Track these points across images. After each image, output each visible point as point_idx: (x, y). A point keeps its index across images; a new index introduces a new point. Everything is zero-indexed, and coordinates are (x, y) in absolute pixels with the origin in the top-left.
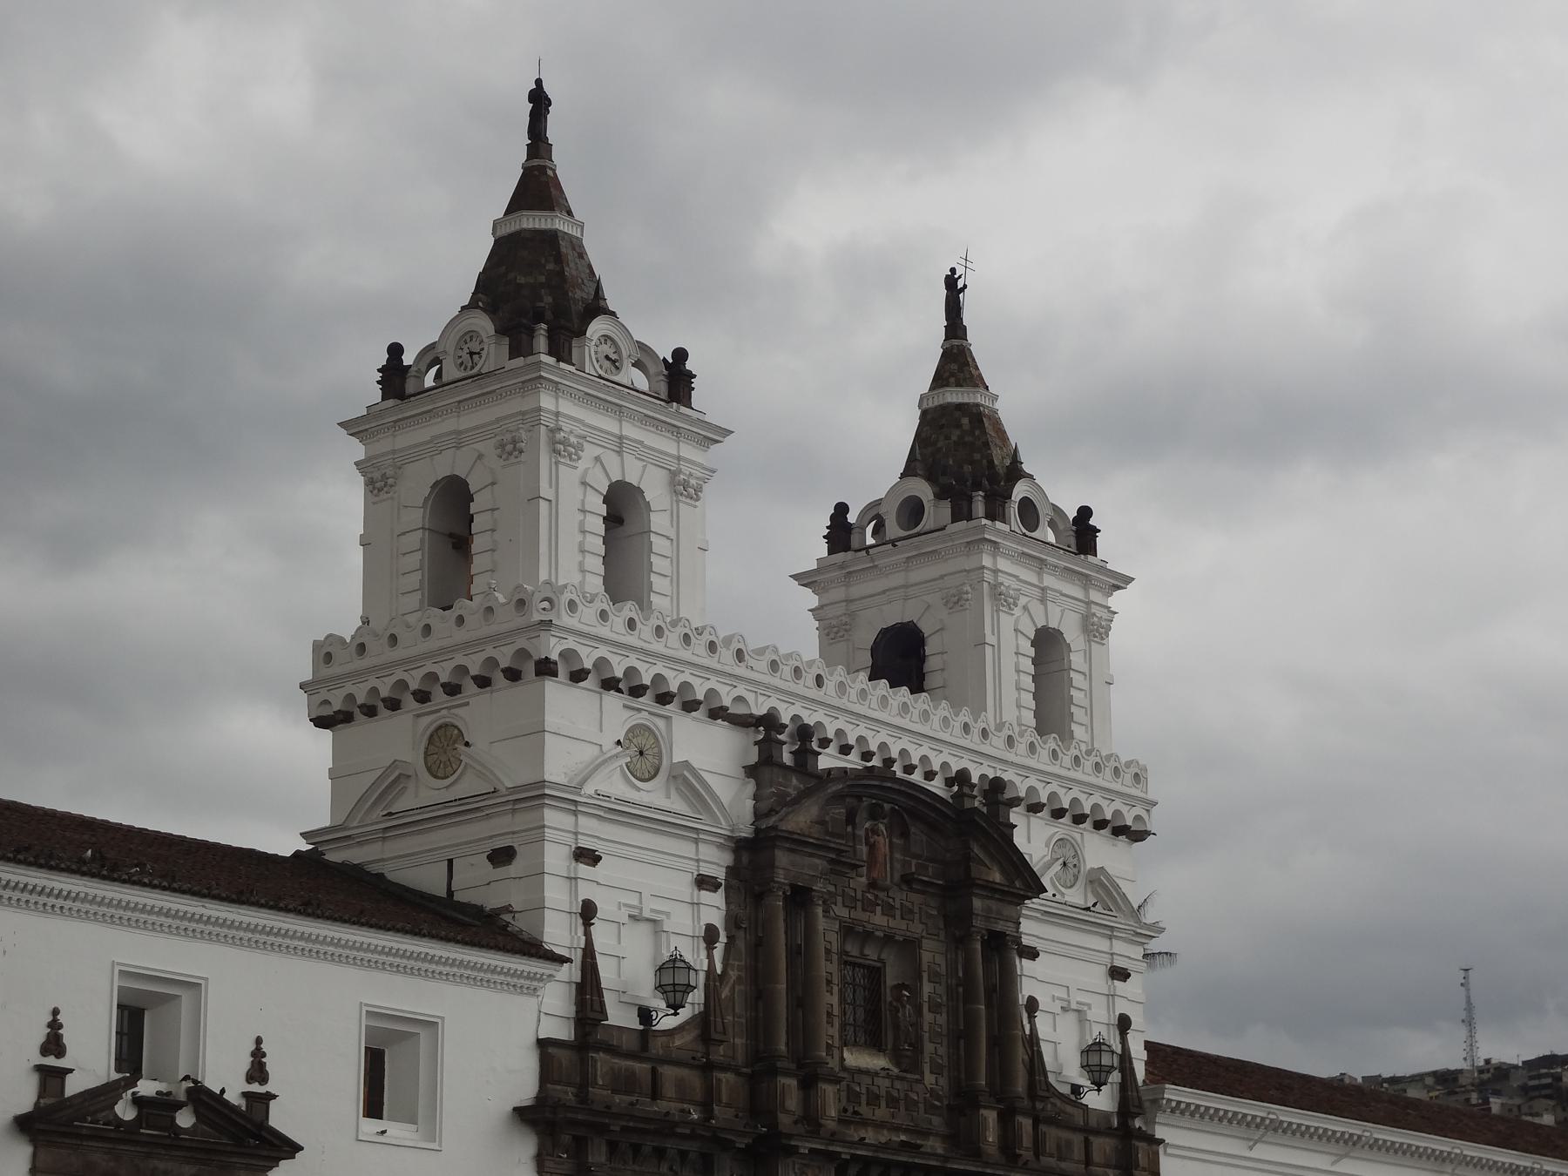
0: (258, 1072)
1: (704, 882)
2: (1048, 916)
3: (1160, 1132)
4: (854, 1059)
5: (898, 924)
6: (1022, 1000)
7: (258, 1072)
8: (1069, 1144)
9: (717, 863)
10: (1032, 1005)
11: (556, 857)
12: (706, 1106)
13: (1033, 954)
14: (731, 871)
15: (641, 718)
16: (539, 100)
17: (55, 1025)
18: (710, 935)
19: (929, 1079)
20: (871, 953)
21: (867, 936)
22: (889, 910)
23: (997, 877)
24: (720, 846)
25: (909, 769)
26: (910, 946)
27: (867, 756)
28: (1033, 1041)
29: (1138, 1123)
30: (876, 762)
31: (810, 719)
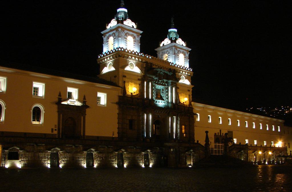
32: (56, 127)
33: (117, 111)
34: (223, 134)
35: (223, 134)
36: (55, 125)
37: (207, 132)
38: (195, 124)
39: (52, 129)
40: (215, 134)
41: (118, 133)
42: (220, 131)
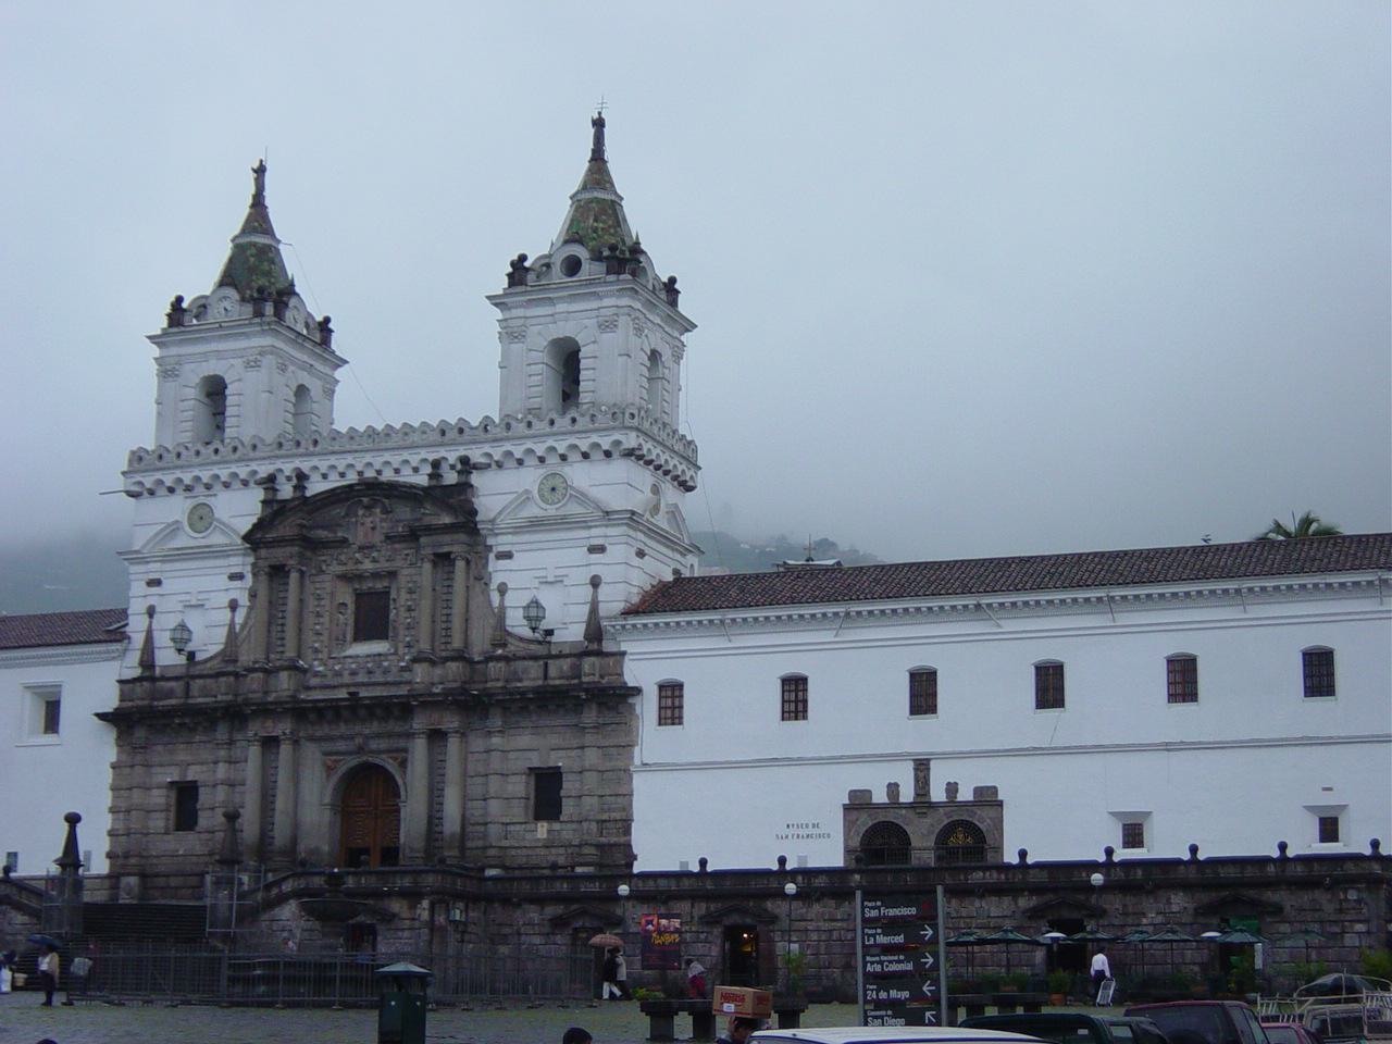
1: (233, 577)
2: (517, 530)
3: (623, 649)
5: (384, 565)
6: (494, 586)
8: (525, 671)
9: (243, 563)
10: (503, 589)
11: (138, 588)
12: (216, 697)
13: (508, 555)
14: (254, 565)
15: (202, 500)
16: (260, 171)
18: (233, 606)
20: (379, 585)
21: (360, 577)
22: (374, 561)
23: (447, 519)
24: (244, 555)
25: (397, 471)
26: (392, 575)
27: (360, 473)
28: (502, 608)
29: (608, 646)
30: (369, 474)
33: (111, 753)
34: (952, 789)
35: (952, 789)
37: (73, 820)
38: (637, 750)
40: (858, 804)
41: (109, 855)
42: (922, 767)
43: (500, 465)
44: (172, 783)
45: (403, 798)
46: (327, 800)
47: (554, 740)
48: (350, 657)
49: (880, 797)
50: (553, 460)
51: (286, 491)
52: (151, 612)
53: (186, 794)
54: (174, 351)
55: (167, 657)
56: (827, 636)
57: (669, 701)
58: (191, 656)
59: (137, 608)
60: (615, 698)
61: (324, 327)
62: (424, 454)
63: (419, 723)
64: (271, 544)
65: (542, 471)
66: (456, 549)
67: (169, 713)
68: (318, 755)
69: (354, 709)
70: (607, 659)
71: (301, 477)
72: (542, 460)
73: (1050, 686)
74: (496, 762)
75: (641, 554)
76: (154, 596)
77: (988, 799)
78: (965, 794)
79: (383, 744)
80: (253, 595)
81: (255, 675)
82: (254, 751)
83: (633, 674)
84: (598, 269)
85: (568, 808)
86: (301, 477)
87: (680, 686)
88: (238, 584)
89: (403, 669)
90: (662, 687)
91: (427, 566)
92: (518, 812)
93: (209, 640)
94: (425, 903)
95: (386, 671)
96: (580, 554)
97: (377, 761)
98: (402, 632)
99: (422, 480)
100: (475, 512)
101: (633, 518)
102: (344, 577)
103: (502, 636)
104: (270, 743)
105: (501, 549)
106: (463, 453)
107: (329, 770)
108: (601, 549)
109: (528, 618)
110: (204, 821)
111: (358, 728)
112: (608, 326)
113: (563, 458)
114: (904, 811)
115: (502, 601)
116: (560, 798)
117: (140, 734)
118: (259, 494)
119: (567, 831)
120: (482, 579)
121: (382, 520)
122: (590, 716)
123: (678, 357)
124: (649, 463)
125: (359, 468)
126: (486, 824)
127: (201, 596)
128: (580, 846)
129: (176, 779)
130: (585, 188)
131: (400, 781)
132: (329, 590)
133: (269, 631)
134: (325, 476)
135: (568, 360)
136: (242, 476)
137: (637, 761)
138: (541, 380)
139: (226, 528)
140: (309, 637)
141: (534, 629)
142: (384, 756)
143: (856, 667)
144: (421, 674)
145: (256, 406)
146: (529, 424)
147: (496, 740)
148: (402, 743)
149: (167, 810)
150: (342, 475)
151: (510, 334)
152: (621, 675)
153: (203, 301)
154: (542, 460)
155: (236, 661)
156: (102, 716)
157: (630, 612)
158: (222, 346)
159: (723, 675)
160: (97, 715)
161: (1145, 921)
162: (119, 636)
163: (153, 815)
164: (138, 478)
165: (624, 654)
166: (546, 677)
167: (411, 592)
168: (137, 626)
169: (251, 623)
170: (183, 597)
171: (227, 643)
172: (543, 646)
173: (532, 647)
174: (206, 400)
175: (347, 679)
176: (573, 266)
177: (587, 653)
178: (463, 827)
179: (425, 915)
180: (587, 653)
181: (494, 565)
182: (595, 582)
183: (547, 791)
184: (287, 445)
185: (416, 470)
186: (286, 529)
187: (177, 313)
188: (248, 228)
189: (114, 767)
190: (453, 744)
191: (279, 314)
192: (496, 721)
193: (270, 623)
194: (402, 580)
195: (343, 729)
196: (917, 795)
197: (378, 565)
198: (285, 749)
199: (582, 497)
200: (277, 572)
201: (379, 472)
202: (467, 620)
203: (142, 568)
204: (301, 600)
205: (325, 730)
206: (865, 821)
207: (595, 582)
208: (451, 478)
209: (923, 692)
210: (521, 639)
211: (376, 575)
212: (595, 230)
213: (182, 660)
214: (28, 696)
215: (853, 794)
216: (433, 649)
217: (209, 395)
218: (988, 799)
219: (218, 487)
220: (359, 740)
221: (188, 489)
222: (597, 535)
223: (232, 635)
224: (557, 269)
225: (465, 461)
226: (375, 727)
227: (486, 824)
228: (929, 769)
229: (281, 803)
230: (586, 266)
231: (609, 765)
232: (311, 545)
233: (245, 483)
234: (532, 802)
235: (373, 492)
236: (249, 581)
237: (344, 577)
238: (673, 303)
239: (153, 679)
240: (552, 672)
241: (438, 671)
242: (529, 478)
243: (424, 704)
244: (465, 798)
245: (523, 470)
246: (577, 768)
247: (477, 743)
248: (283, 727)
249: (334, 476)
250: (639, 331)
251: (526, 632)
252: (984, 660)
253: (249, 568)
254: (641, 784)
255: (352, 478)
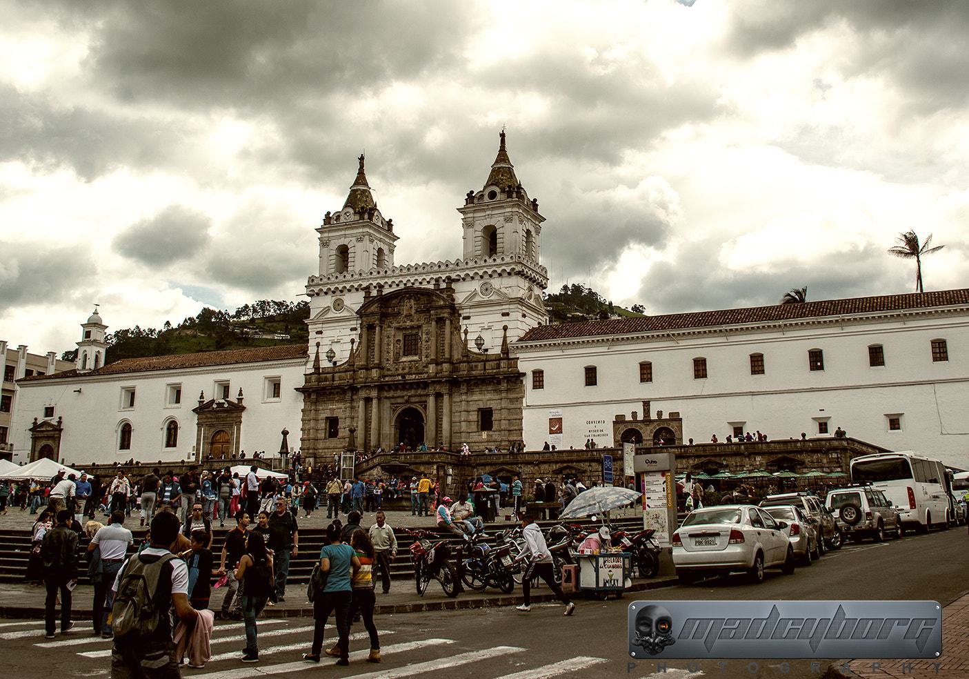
0: (241, 394)
1: (352, 330)
2: (471, 307)
4: (404, 359)
7: (241, 394)
8: (476, 366)
9: (356, 323)
10: (466, 332)
11: (312, 335)
13: (468, 318)
15: (339, 297)
17: (202, 393)
18: (353, 341)
19: (424, 359)
20: (414, 332)
21: (405, 329)
22: (412, 321)
23: (442, 303)
25: (421, 283)
26: (419, 327)
27: (405, 284)
28: (466, 340)
29: (511, 356)
31: (382, 282)
32: (193, 451)
34: (660, 413)
35: (660, 413)
36: (194, 447)
37: (285, 433)
38: (524, 399)
39: (189, 454)
40: (619, 420)
42: (646, 404)
43: (464, 279)
44: (327, 418)
45: (425, 422)
46: (393, 424)
47: (488, 396)
48: (402, 362)
49: (629, 418)
50: (486, 277)
51: (374, 293)
52: (318, 345)
53: (333, 422)
54: (326, 235)
55: (325, 364)
56: (604, 349)
57: (538, 379)
58: (335, 363)
59: (312, 343)
60: (517, 377)
61: (389, 223)
62: (432, 276)
63: (431, 390)
64: (367, 315)
65: (482, 282)
66: (446, 315)
67: (324, 388)
68: (389, 405)
69: (405, 386)
70: (510, 361)
71: (381, 287)
72: (482, 277)
73: (700, 368)
74: (464, 406)
75: (524, 316)
76: (319, 338)
77: (675, 417)
78: (665, 416)
79: (417, 399)
80: (361, 336)
81: (362, 371)
82: (361, 403)
83: (522, 367)
84: (504, 196)
85: (495, 427)
86: (381, 287)
87: (542, 372)
88: (354, 332)
89: (425, 367)
90: (534, 372)
91: (434, 323)
92: (474, 427)
93: (343, 355)
94: (435, 467)
95: (417, 368)
96: (499, 317)
97: (414, 407)
98: (424, 351)
99: (431, 287)
100: (453, 300)
101: (520, 301)
102: (398, 329)
103: (467, 353)
104: (368, 400)
105: (465, 315)
106: (448, 275)
107: (394, 410)
108: (507, 314)
109: (477, 344)
110: (340, 434)
111: (405, 393)
112: (508, 220)
113: (491, 276)
114: (639, 424)
115: (466, 337)
116: (492, 422)
117: (313, 397)
118: (362, 294)
119: (496, 436)
120: (458, 328)
121: (415, 304)
122: (504, 386)
123: (538, 233)
124: (526, 277)
125: (405, 282)
126: (461, 433)
127: (339, 338)
128: (501, 441)
129: (330, 416)
130: (497, 162)
131: (424, 415)
132: (393, 334)
133: (368, 352)
134: (390, 286)
135: (491, 235)
136: (356, 287)
137: (524, 405)
138: (479, 245)
139: (349, 309)
140: (385, 355)
141: (479, 349)
142: (417, 405)
143: (618, 363)
144: (432, 369)
145: (362, 259)
146: (476, 262)
147: (464, 397)
148: (423, 399)
149: (326, 429)
150: (398, 285)
151: (467, 224)
152: (517, 367)
153: (338, 214)
154: (482, 277)
155: (354, 365)
156: (297, 389)
157: (521, 340)
158: (347, 232)
159: (561, 367)
160: (296, 389)
161: (745, 469)
162: (304, 353)
163: (320, 432)
164: (312, 288)
165: (518, 358)
166: (485, 369)
167: (427, 334)
168: (312, 351)
169: (360, 348)
170: (330, 339)
171: (350, 358)
172: (485, 359)
173: (479, 356)
174: (340, 255)
175: (400, 371)
176: (493, 195)
177: (501, 359)
178: (451, 436)
179: (435, 472)
180: (504, 359)
181: (463, 323)
182: (505, 328)
183: (486, 419)
184: (374, 274)
185: (428, 282)
186: (374, 308)
187: (328, 218)
188: (356, 183)
189: (302, 411)
190: (446, 398)
191: (371, 216)
192: (464, 388)
193: (368, 348)
194: (424, 329)
195: (399, 393)
196: (644, 417)
197: (413, 323)
198: (375, 402)
199: (498, 292)
200: (371, 328)
201: (413, 284)
202: (451, 346)
203: (314, 326)
204: (381, 339)
205: (391, 394)
206: (623, 428)
207: (505, 328)
208: (443, 285)
209: (646, 372)
210: (475, 353)
211: (412, 328)
212: (502, 180)
213: (331, 365)
214: (267, 381)
215: (617, 416)
216: (437, 357)
217: (341, 253)
218: (675, 417)
219: (346, 291)
220: (406, 398)
221: (334, 292)
222: (505, 308)
223: (352, 354)
224: (486, 197)
225: (449, 278)
226: (413, 392)
227: (461, 433)
228: (649, 405)
229: (374, 425)
230: (498, 195)
231: (513, 406)
232: (384, 316)
233: (357, 290)
234: (480, 423)
235: (410, 293)
236: (359, 331)
237: (398, 329)
238: (536, 210)
239: (319, 374)
240: (487, 368)
241: (439, 367)
242: (476, 285)
243: (433, 382)
244: (451, 422)
245: (473, 281)
246: (499, 407)
247: (456, 399)
248: (374, 394)
249: (394, 286)
250: (521, 222)
251: (476, 351)
252: (671, 361)
253: (359, 326)
254: (525, 413)
255: (402, 286)
